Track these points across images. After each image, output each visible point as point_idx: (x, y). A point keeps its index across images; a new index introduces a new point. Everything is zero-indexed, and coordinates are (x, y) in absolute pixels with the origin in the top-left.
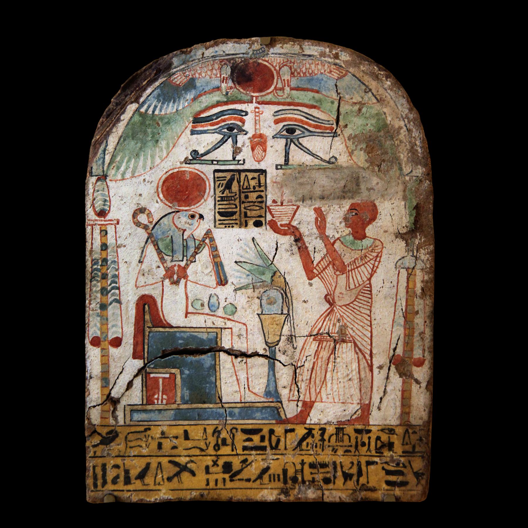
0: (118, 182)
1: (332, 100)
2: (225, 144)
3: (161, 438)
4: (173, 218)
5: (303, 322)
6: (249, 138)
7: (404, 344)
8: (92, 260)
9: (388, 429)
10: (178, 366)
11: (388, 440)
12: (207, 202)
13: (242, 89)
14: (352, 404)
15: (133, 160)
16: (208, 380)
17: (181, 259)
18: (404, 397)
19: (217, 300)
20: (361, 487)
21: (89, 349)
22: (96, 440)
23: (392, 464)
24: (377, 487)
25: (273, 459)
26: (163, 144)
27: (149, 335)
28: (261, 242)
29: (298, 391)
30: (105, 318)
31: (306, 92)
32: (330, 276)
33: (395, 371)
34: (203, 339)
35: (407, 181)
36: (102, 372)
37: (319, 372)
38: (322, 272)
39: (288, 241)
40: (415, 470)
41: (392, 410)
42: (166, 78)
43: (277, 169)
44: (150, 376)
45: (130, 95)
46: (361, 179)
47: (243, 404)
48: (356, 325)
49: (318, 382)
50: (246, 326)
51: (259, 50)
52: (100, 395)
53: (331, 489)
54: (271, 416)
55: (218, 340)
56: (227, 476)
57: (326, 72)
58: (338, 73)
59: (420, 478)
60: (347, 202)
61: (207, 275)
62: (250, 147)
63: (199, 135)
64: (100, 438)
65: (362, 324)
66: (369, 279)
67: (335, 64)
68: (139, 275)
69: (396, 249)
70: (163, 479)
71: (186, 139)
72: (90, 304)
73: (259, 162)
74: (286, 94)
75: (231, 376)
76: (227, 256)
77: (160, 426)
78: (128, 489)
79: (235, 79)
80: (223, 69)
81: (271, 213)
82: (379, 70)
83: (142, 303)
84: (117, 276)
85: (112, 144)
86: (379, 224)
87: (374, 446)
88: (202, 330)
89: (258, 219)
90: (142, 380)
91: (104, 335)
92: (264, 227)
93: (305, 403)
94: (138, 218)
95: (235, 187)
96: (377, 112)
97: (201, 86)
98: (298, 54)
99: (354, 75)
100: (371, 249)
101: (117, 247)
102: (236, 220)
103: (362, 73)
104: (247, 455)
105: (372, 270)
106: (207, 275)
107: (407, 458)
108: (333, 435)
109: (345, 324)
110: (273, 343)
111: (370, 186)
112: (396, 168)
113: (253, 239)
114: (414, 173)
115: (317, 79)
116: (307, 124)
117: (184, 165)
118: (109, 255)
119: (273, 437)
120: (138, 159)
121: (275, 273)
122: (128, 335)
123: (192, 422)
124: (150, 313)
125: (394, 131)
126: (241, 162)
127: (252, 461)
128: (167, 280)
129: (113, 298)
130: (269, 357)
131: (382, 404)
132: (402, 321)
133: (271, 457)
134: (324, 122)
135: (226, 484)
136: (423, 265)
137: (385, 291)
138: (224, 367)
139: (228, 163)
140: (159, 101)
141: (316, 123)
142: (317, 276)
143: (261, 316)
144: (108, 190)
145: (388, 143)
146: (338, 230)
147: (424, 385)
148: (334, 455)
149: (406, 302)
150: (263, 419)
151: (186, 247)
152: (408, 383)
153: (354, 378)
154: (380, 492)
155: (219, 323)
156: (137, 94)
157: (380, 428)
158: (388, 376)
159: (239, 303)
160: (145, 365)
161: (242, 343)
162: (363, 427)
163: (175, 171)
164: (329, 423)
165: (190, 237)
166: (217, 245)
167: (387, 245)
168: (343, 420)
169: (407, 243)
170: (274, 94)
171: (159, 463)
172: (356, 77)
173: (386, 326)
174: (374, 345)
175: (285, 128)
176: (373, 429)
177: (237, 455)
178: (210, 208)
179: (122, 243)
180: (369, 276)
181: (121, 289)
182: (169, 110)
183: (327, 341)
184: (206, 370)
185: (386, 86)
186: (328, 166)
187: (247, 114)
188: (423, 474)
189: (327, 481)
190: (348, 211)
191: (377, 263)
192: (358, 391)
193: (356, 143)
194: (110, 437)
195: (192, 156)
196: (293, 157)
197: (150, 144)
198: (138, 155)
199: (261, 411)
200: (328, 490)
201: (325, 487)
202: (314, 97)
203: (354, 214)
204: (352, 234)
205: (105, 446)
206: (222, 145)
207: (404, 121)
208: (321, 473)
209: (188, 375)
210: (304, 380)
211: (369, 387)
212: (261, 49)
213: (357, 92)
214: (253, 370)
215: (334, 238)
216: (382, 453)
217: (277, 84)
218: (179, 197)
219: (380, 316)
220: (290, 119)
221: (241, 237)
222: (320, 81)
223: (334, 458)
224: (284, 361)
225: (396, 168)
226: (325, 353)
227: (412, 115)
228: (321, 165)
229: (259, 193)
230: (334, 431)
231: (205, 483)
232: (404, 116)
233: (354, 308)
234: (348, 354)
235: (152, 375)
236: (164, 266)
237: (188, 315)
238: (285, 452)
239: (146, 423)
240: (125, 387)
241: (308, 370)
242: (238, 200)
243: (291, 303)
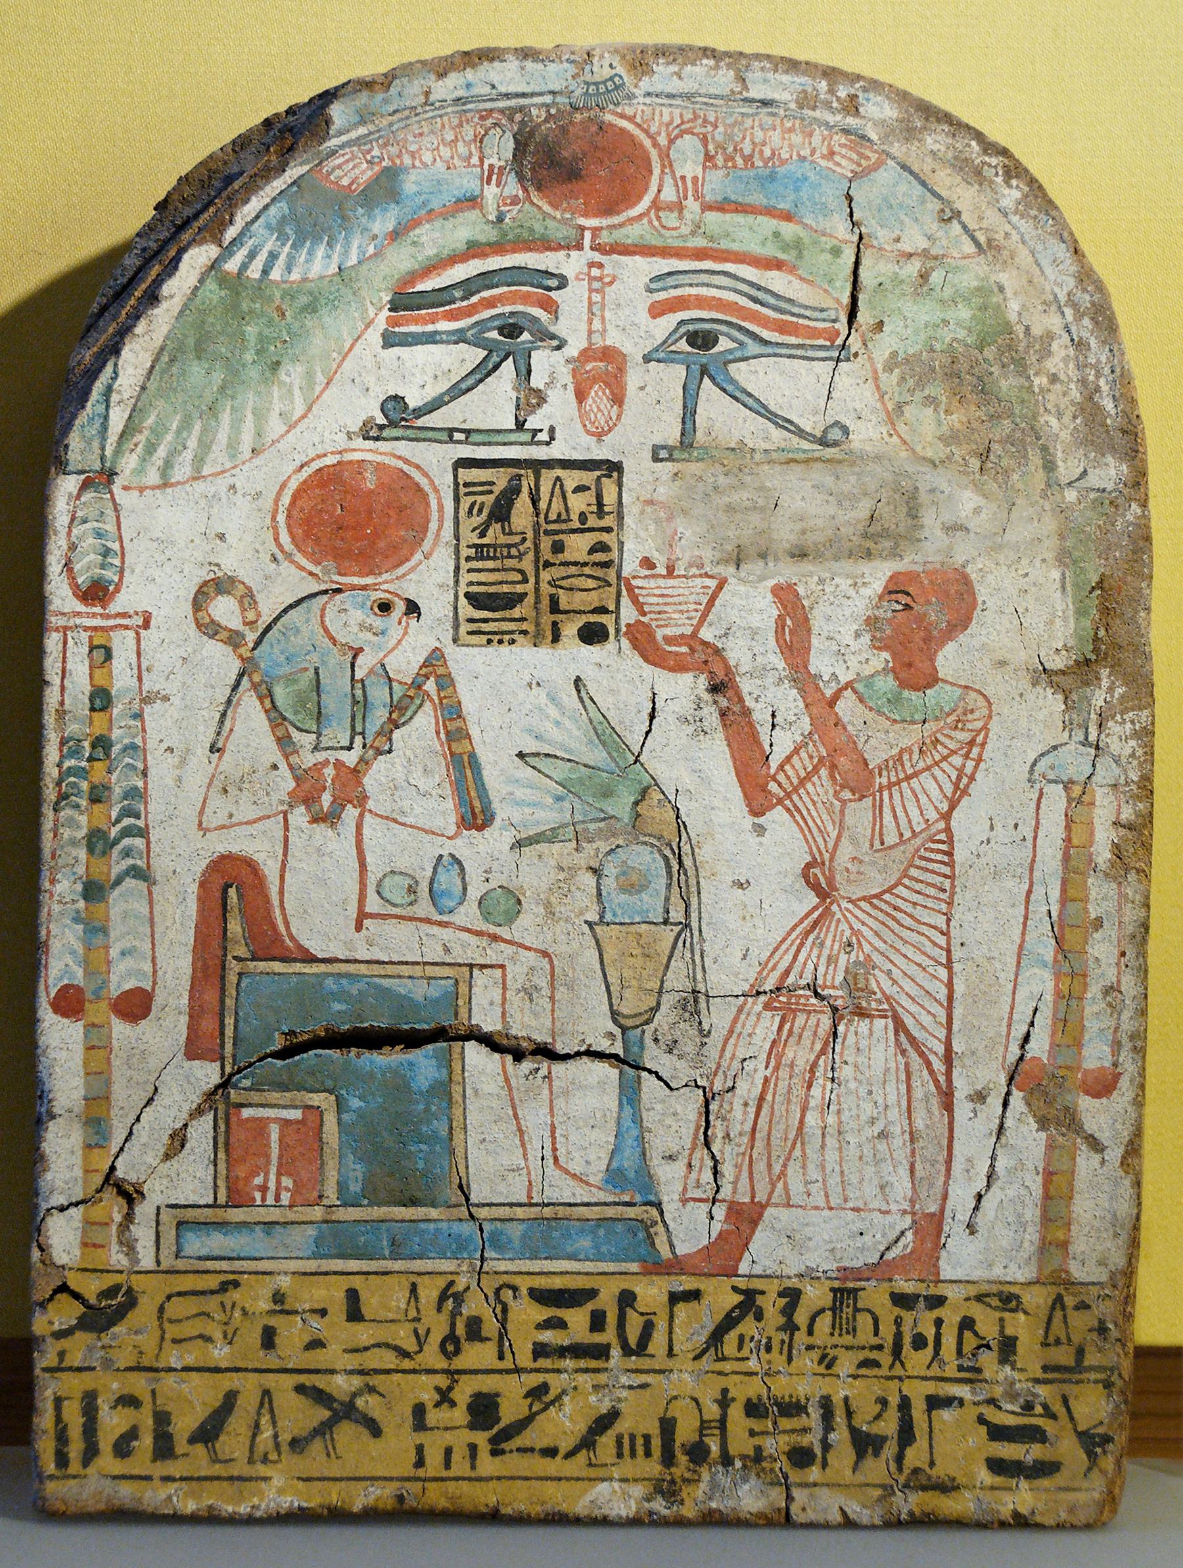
0: (148, 492)
3: (273, 1312)
4: (323, 610)
7: (1054, 1024)
8: (63, 743)
9: (999, 1295)
13: (551, 204)
14: (887, 1212)
15: (197, 427)
20: (908, 1480)
21: (46, 1024)
22: (64, 1313)
23: (1009, 1407)
24: (961, 1480)
26: (292, 374)
27: (238, 985)
29: (716, 1172)
32: (819, 805)
38: (796, 790)
43: (656, 459)
46: (923, 497)
50: (551, 962)
52: (78, 1172)
53: (815, 1485)
55: (460, 1002)
56: (481, 1438)
57: (818, 154)
58: (854, 156)
59: (1098, 1450)
62: (571, 387)
65: (919, 958)
66: (947, 816)
67: (846, 131)
70: (277, 1446)
72: (53, 881)
73: (600, 435)
77: (270, 1273)
78: (165, 1474)
83: (217, 882)
85: (131, 371)
86: (976, 643)
87: (954, 1347)
89: (593, 618)
90: (216, 1126)
92: (611, 645)
93: (734, 1210)
95: (522, 515)
96: (975, 284)
99: (904, 167)
100: (953, 717)
101: (143, 701)
102: (522, 619)
103: (929, 160)
104: (547, 1371)
105: (956, 786)
108: (823, 1310)
109: (868, 957)
111: (947, 517)
114: (1093, 480)
117: (359, 443)
119: (631, 1315)
121: (644, 792)
123: (373, 1265)
126: (543, 436)
127: (564, 1392)
131: (980, 1214)
132: (1048, 950)
133: (624, 1380)
134: (808, 313)
135: (478, 1462)
136: (1117, 771)
140: (282, 238)
142: (780, 802)
144: (118, 518)
147: (1114, 1154)
148: (823, 1375)
149: (1064, 891)
151: (360, 705)
157: (972, 1291)
163: (330, 460)
164: (809, 1275)
165: (376, 674)
170: (650, 222)
171: (266, 1393)
172: (911, 173)
176: (951, 1292)
177: (518, 1370)
178: (440, 580)
180: (945, 807)
183: (809, 1012)
186: (817, 454)
187: (563, 283)
188: (1107, 1439)
189: (801, 1457)
190: (881, 598)
192: (904, 1172)
195: (386, 416)
198: (213, 410)
199: (593, 1232)
200: (805, 1485)
201: (795, 1476)
204: (893, 670)
205: (94, 1335)
206: (481, 381)
208: (784, 1432)
212: (611, 79)
215: (838, 682)
220: (701, 302)
223: (825, 1387)
230: (828, 1302)
231: (412, 1457)
232: (1063, 298)
235: (246, 1113)
237: (367, 922)
239: (224, 1266)
241: (746, 1104)
242: (531, 556)
243: (694, 889)
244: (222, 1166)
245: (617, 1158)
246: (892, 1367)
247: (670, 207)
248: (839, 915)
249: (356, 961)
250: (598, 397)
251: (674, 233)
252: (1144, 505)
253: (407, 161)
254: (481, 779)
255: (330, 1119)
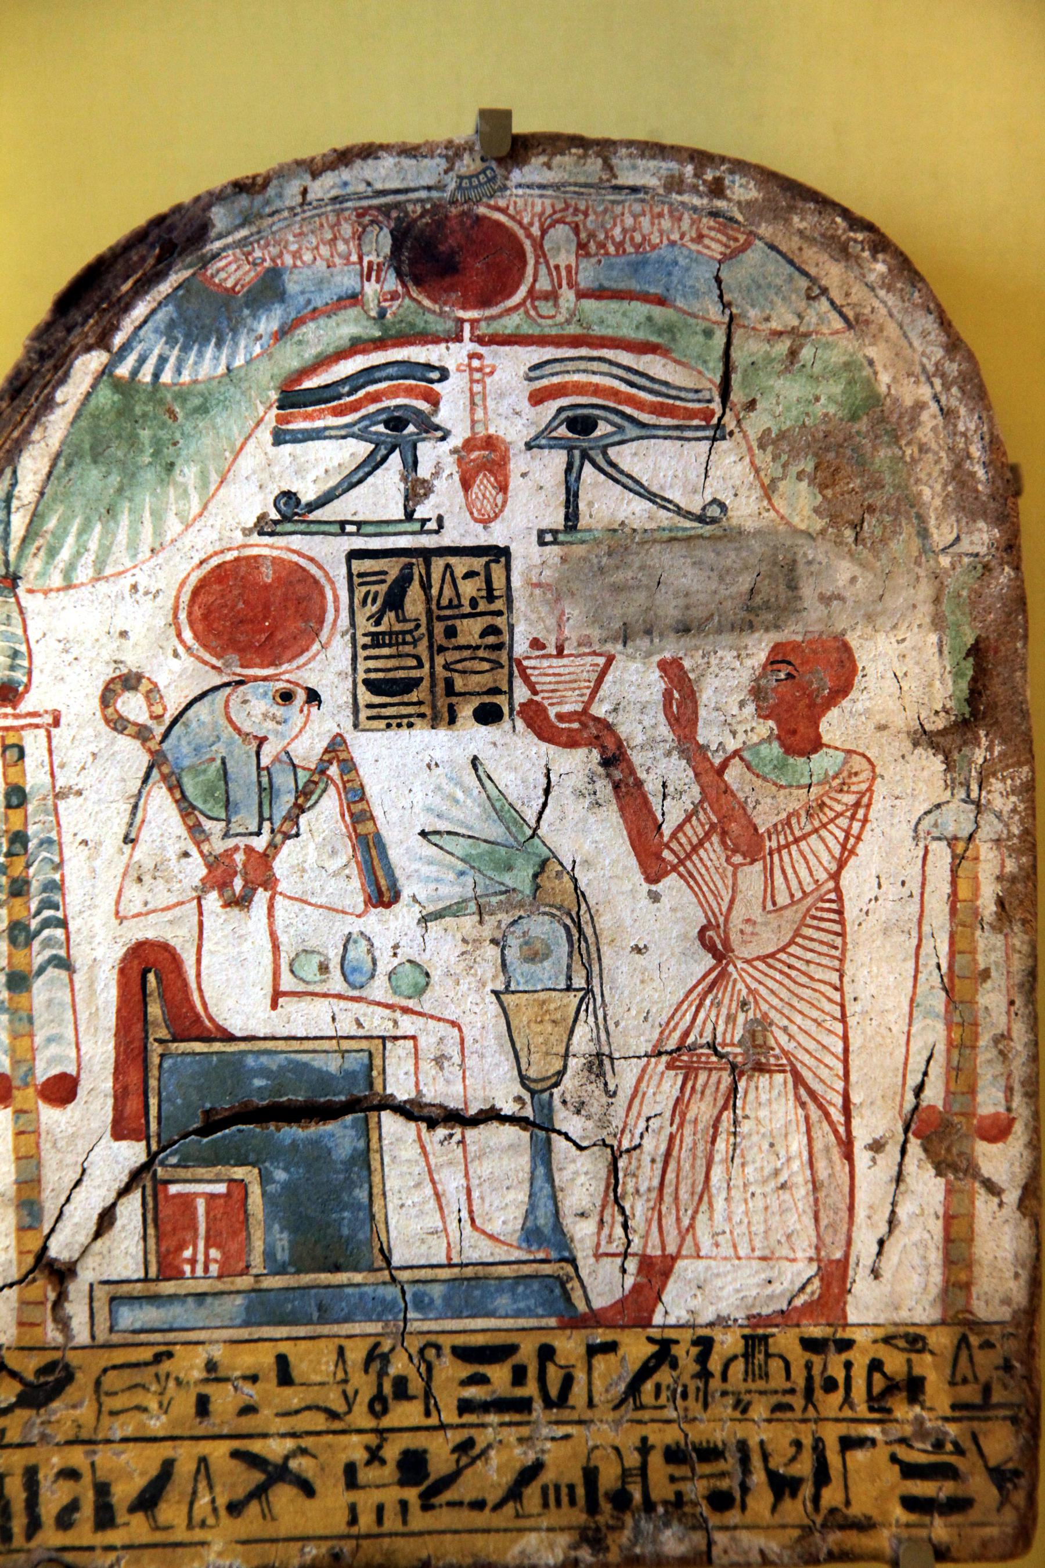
0: (53, 595)
1: (705, 324)
2: (378, 472)
3: (206, 1381)
4: (227, 702)
5: (633, 1012)
6: (454, 451)
7: (948, 1073)
9: (906, 1336)
10: (252, 1157)
11: (905, 1369)
12: (330, 652)
13: (429, 297)
14: (793, 1260)
15: (98, 528)
16: (345, 1197)
17: (254, 828)
18: (953, 1236)
19: (369, 951)
20: (825, 1519)
23: (919, 1445)
24: (877, 1517)
25: (553, 1439)
26: (188, 474)
27: (160, 1066)
28: (500, 769)
29: (625, 1226)
30: (24, 1014)
31: (625, 304)
32: (712, 870)
33: (923, 1156)
34: (327, 1072)
35: (946, 571)
36: (20, 1183)
37: (686, 1166)
38: (688, 856)
39: (580, 767)
40: (992, 1463)
41: (916, 1277)
42: (190, 272)
43: (542, 543)
44: (166, 1190)
45: (83, 324)
46: (802, 569)
47: (456, 1270)
48: (798, 1019)
49: (684, 1195)
50: (460, 1030)
51: (477, 176)
52: (13, 1254)
53: (735, 1527)
54: (543, 1305)
55: (374, 1073)
56: (412, 1494)
57: (687, 238)
58: (724, 239)
59: (1010, 1486)
60: (760, 641)
61: (335, 875)
62: (457, 477)
63: (298, 446)
64: (18, 1387)
65: (815, 1014)
66: (835, 876)
67: (714, 214)
68: (128, 880)
69: (915, 779)
70: (215, 1510)
71: (261, 458)
74: (563, 311)
75: (418, 1185)
76: (394, 815)
79: (405, 268)
80: (366, 239)
81: (526, 679)
82: (851, 228)
83: (136, 967)
84: (57, 887)
85: (30, 477)
86: (859, 706)
88: (326, 1045)
89: (487, 699)
90: (144, 1204)
91: (24, 1068)
92: (506, 724)
93: (646, 1263)
94: (119, 705)
95: (414, 603)
96: (845, 358)
97: (303, 292)
98: (597, 186)
99: (772, 247)
100: (838, 781)
101: (56, 796)
102: (420, 703)
103: (796, 238)
104: (472, 1426)
105: (844, 847)
106: (335, 875)
107: (965, 1425)
108: (735, 1357)
109: (765, 1015)
110: (543, 1079)
111: (828, 590)
112: (908, 529)
113: (475, 762)
114: (965, 546)
115: (661, 261)
116: (631, 400)
117: (255, 538)
118: (30, 821)
120: (112, 524)
121: (544, 864)
122: (97, 1068)
123: (301, 1331)
124: (162, 996)
125: (900, 417)
126: (432, 525)
127: (489, 1446)
128: (214, 895)
129: (48, 953)
130: (534, 1124)
131: (884, 1258)
132: (938, 1001)
133: (545, 1431)
134: (683, 394)
135: (410, 1518)
136: (1000, 827)
137: (884, 910)
138: (394, 1158)
139: (391, 529)
140: (171, 341)
141: (660, 399)
142: (674, 868)
143: (507, 998)
144: (24, 620)
145: (882, 453)
146: (735, 727)
147: (1012, 1197)
149: (952, 943)
150: (518, 1314)
151: (267, 792)
152: (962, 1191)
153: (795, 1179)
154: (886, 1533)
155: (377, 1022)
156: (104, 322)
157: (880, 1333)
158: (900, 1173)
159: (435, 958)
160: (152, 1157)
161: (448, 1082)
162: (829, 1331)
163: (229, 556)
164: (721, 1322)
166: (365, 782)
167: (889, 769)
168: (766, 1311)
169: (948, 761)
170: (527, 312)
171: (203, 1460)
172: (779, 252)
173: (892, 1017)
174: (853, 1078)
175: (563, 416)
176: (860, 1336)
177: (442, 1427)
178: (340, 668)
179: (72, 782)
180: (833, 867)
181: (72, 926)
182: (205, 369)
183: (710, 1070)
184: (339, 1166)
185: (872, 277)
187: (444, 375)
189: (720, 1501)
190: (764, 667)
191: (856, 826)
192: (808, 1221)
193: (784, 457)
194: (47, 1383)
195: (279, 511)
196: (590, 504)
197: (149, 476)
199: (513, 1290)
200: (725, 1528)
201: (714, 1520)
202: (649, 319)
203: (782, 676)
204: (778, 738)
205: (32, 1413)
206: (369, 474)
207: (932, 385)
208: (701, 1477)
209: (286, 1186)
210: (643, 1189)
211: (844, 1206)
212: (484, 171)
213: (784, 299)
214: (485, 1164)
216: (889, 1411)
217: (535, 280)
218: (242, 638)
219: (872, 989)
220: (579, 389)
221: (438, 755)
222: (667, 267)
223: (741, 1431)
224: (580, 1133)
225: (908, 529)
226: (703, 1108)
227: (955, 366)
228: (678, 529)
229: (489, 620)
230: (739, 1347)
231: (343, 1516)
232: (931, 369)
233: (790, 967)
234: (775, 1106)
235: (173, 1189)
236: (201, 852)
237: (281, 1001)
238: (588, 1415)
240: (92, 1227)
241: (653, 1161)
242: (424, 643)
243: (595, 956)
244: (152, 1242)
245: (531, 1217)
246: (805, 1409)
247: (547, 296)
248: (735, 975)
249: (274, 1038)
250: (484, 485)
251: (549, 322)
252: (1017, 568)
253: (288, 260)
254: (386, 857)
255: (255, 1191)
